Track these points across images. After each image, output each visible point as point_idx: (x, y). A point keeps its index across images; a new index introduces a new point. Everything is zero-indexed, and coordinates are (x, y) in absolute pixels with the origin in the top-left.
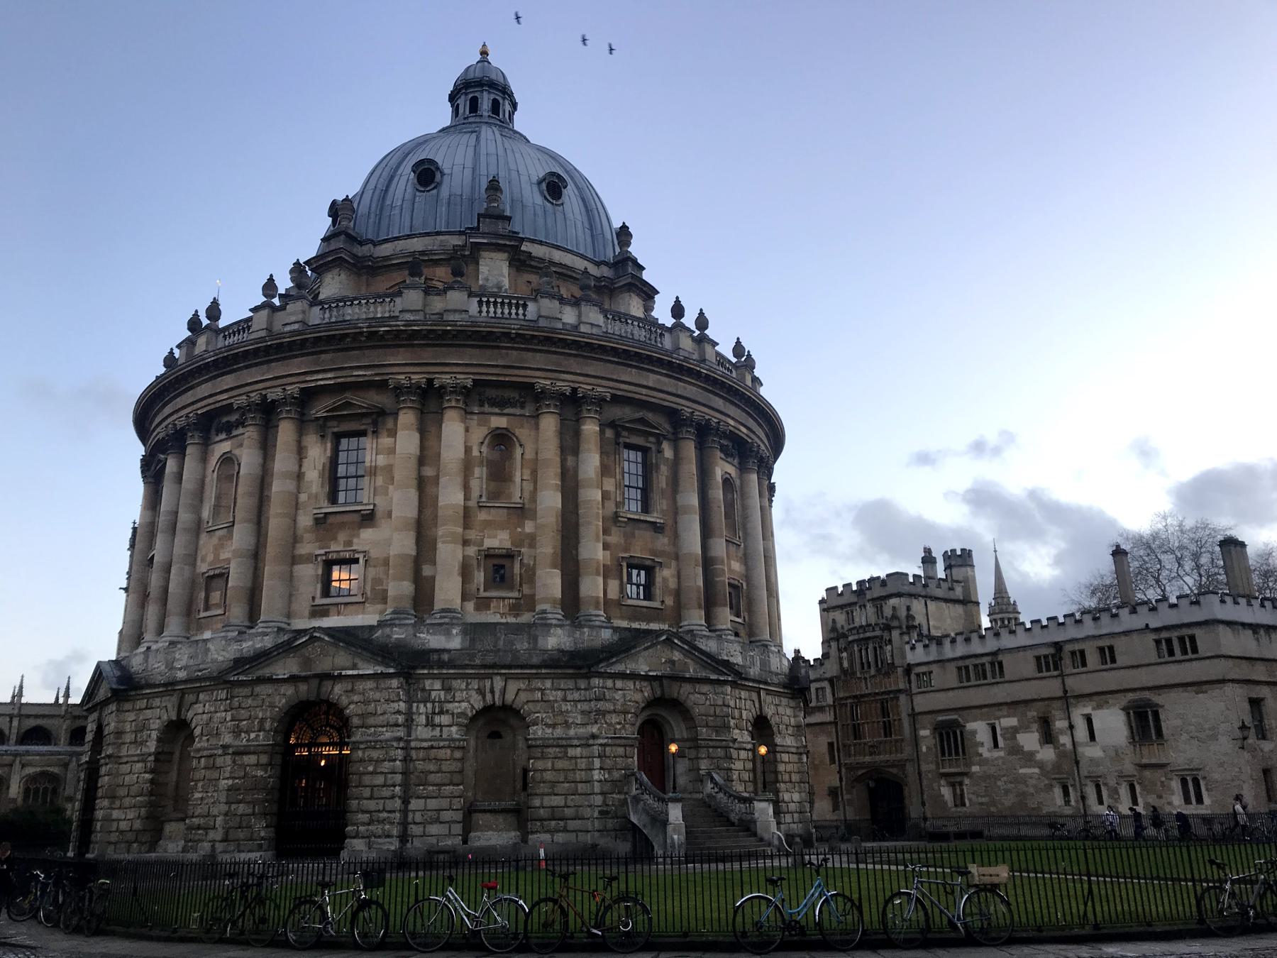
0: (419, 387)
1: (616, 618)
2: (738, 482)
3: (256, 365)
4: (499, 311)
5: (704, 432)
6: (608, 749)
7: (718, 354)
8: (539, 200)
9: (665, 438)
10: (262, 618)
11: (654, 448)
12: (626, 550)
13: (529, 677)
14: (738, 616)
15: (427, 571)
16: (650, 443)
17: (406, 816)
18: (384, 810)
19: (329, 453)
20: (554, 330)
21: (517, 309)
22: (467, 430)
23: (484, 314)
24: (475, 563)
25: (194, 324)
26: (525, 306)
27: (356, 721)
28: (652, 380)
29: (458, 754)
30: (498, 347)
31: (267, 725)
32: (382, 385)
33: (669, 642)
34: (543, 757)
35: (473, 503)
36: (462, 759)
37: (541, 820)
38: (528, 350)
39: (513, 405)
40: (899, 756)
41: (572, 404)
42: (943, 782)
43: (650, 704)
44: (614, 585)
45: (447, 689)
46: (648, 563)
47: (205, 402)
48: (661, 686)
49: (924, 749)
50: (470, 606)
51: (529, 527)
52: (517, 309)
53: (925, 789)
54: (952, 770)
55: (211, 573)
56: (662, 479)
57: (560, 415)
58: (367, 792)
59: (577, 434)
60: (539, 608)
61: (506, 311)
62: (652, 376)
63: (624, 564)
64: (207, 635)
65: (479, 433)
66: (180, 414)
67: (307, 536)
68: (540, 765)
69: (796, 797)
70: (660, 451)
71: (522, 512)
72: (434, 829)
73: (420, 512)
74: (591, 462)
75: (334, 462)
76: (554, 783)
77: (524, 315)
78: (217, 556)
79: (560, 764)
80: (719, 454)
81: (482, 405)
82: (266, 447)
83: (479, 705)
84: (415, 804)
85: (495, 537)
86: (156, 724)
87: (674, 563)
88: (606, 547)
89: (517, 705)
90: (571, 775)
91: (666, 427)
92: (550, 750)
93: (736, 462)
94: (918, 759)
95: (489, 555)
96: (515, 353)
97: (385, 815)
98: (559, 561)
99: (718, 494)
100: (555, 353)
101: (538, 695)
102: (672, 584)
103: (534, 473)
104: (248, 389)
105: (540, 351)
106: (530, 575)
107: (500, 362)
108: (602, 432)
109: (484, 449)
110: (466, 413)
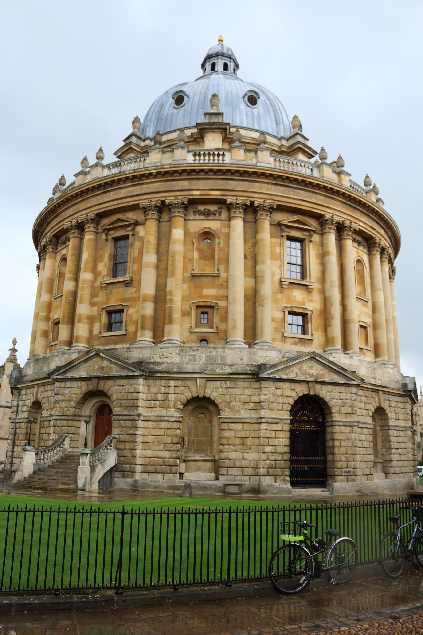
1: (96, 346)
6: (58, 422)
9: (137, 223)
11: (131, 233)
13: (44, 384)
14: (212, 327)
17: (13, 455)
28: (123, 193)
33: (97, 355)
41: (81, 227)
43: (89, 395)
45: (26, 394)
46: (118, 308)
50: (48, 351)
63: (104, 312)
69: (252, 455)
83: (32, 401)
85: (56, 313)
88: (93, 304)
89: (40, 401)
93: (224, 215)
100: (75, 204)
101: (45, 394)
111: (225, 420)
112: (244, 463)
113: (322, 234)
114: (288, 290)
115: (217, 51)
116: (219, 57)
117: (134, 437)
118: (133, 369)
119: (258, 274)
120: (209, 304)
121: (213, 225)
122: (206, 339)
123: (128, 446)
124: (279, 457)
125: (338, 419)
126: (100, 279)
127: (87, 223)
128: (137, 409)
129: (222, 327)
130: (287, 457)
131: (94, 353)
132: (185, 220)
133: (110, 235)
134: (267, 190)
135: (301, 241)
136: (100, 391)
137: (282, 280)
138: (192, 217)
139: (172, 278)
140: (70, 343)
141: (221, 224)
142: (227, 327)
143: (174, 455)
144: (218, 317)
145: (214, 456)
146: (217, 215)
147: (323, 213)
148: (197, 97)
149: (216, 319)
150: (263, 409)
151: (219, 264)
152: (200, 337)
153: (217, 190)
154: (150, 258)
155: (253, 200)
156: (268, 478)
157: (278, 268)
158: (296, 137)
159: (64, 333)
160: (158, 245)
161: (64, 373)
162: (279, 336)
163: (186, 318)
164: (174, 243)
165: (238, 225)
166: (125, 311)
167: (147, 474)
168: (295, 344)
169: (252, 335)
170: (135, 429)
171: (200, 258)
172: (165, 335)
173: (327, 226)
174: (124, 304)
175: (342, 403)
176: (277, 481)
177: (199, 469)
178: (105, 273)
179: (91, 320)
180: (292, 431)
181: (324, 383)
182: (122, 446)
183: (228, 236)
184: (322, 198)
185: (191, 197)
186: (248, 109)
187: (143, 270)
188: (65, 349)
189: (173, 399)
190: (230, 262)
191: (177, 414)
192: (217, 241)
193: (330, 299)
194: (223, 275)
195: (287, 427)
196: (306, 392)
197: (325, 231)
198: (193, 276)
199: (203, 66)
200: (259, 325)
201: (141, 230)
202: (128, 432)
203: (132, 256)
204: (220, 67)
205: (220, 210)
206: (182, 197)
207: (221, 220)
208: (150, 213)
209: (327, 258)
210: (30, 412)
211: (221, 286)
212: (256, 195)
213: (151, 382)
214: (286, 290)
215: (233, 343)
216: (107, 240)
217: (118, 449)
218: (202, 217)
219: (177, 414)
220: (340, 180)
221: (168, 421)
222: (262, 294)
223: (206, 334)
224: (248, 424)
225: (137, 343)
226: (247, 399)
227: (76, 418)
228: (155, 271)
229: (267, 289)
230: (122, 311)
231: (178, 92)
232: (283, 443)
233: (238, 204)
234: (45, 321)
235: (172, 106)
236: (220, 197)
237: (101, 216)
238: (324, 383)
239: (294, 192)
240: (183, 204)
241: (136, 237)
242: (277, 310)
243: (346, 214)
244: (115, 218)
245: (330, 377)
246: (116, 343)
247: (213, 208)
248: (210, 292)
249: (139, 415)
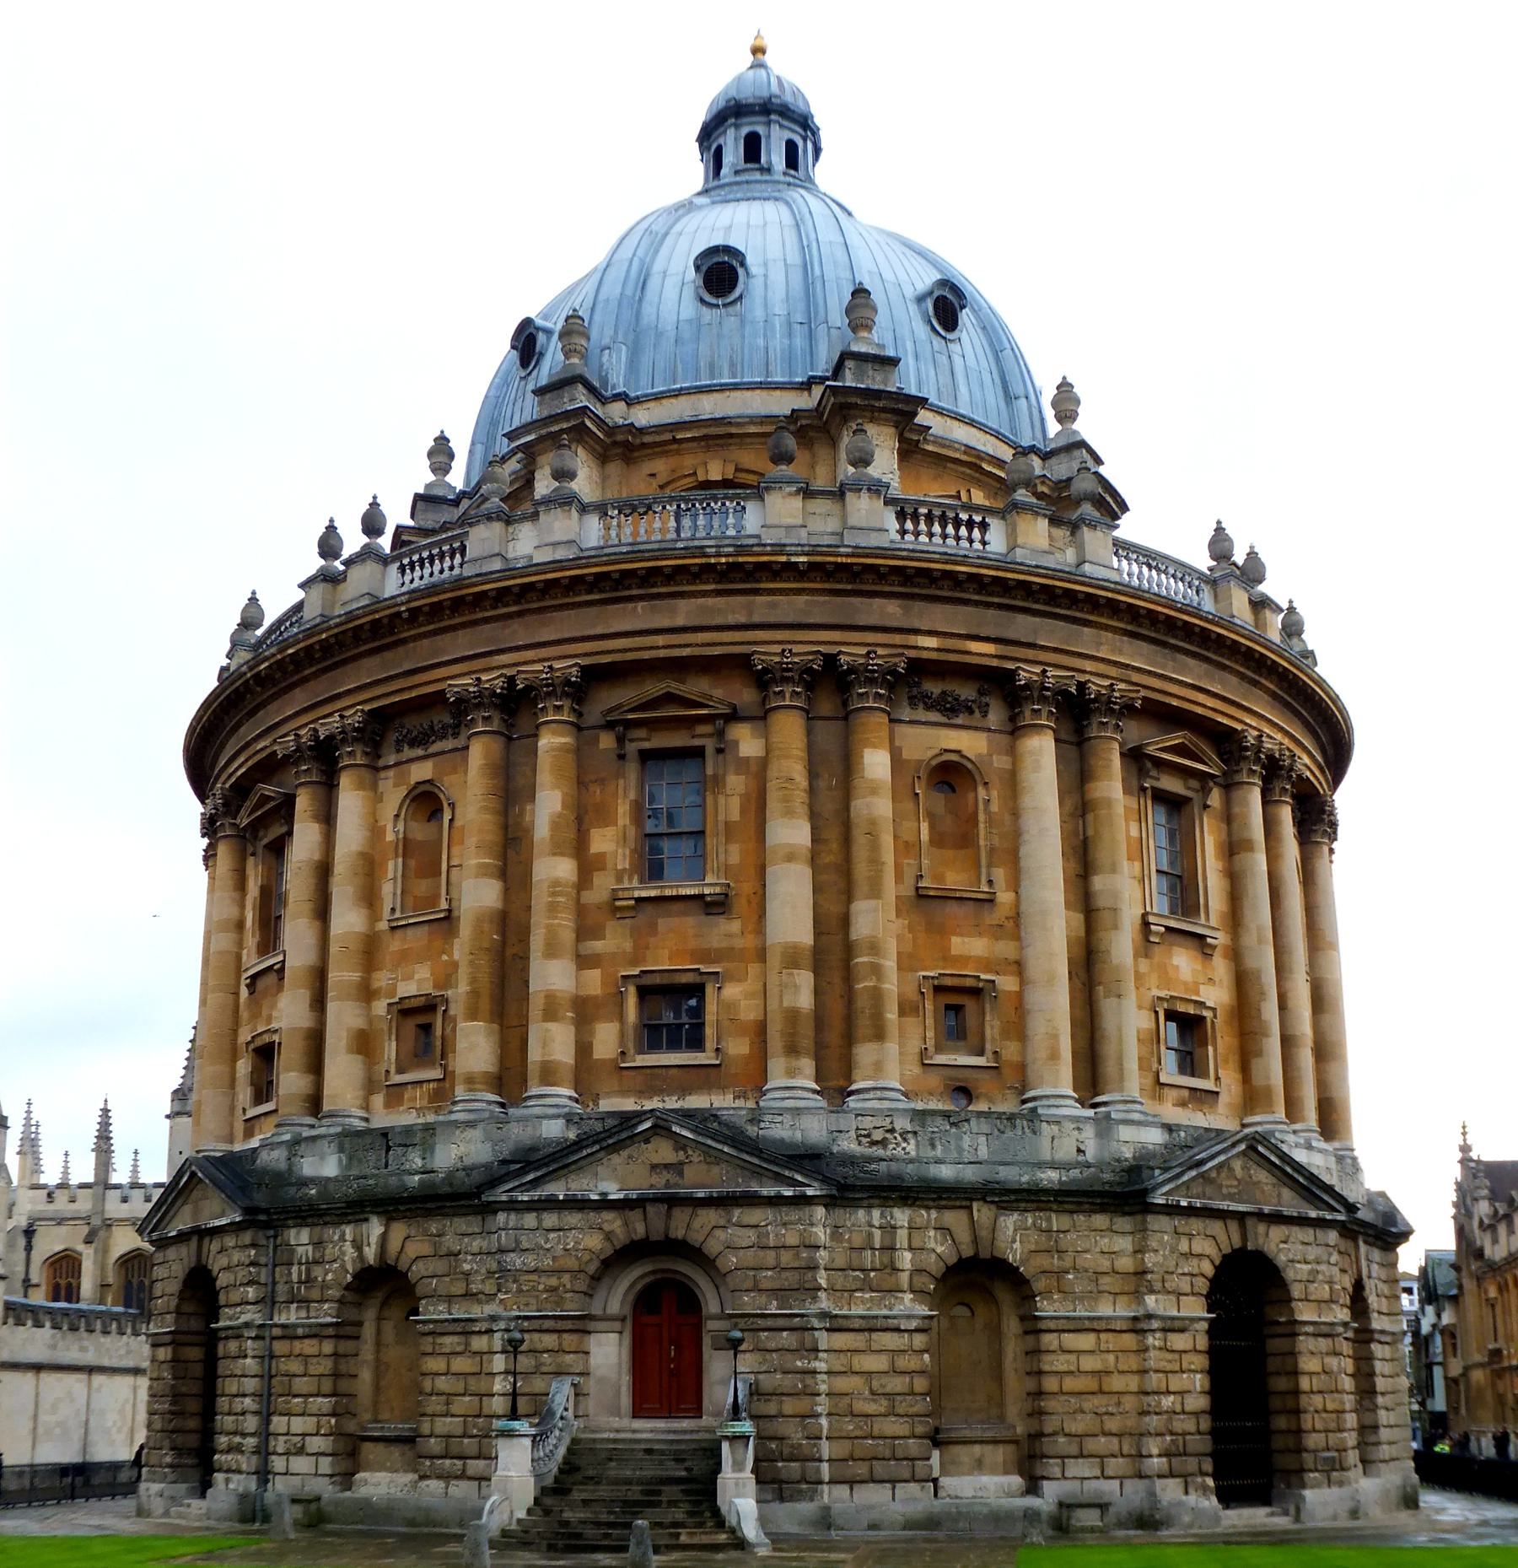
1: (609, 1095)
8: (690, 307)
9: (734, 716)
11: (710, 745)
12: (634, 962)
14: (981, 1053)
16: (702, 738)
28: (683, 612)
39: (443, 737)
56: (730, 804)
62: (683, 605)
63: (632, 990)
65: (393, 795)
79: (461, 1364)
85: (409, 978)
87: (753, 969)
88: (584, 962)
90: (472, 1381)
92: (448, 1340)
93: (996, 716)
96: (426, 642)
98: (485, 1004)
100: (486, 620)
105: (463, 625)
107: (407, 667)
109: (401, 827)
111: (1052, 1325)
112: (1101, 1444)
113: (1229, 786)
114: (1162, 947)
115: (765, 94)
116: (773, 117)
117: (809, 1380)
118: (799, 1178)
119: (1101, 902)
120: (969, 983)
121: (968, 743)
122: (969, 1086)
123: (789, 1406)
124: (1190, 1426)
125: (1305, 1318)
126: (602, 886)
127: (548, 694)
128: (815, 1298)
129: (1010, 1051)
130: (1206, 1423)
131: (647, 1125)
132: (891, 721)
133: (631, 740)
134: (1113, 651)
135: (1173, 804)
136: (676, 1241)
137: (1151, 919)
138: (906, 713)
139: (873, 902)
140: (510, 1080)
141: (989, 741)
142: (1023, 1051)
143: (920, 1430)
144: (997, 1023)
145: (1014, 1427)
146: (977, 714)
147: (1239, 727)
148: (777, 277)
149: (992, 1028)
150: (1152, 1292)
151: (990, 865)
152: (951, 1079)
153: (987, 639)
154: (791, 832)
155: (1083, 678)
156: (1171, 1482)
157: (1136, 884)
158: (1076, 453)
159: (474, 1047)
160: (812, 791)
161: (535, 1183)
162: (1149, 1081)
163: (912, 1022)
164: (874, 791)
165: (1042, 751)
166: (710, 991)
167: (846, 1488)
168: (1182, 1104)
169: (1092, 1077)
170: (813, 1356)
171: (931, 841)
172: (856, 1074)
173: (1244, 766)
174: (703, 969)
175: (1311, 1272)
176: (1191, 1490)
177: (979, 1466)
178: (623, 863)
179: (584, 1012)
180: (1212, 1352)
181: (1277, 1218)
182: (771, 1408)
183: (1013, 783)
184: (1235, 680)
185: (912, 654)
186: (937, 341)
187: (768, 870)
188: (489, 1103)
189: (908, 1266)
190: (1023, 863)
191: (923, 1310)
192: (982, 793)
193: (1259, 978)
194: (1005, 897)
195: (1203, 1342)
196: (1237, 1242)
197: (1237, 778)
198: (921, 896)
199: (708, 135)
200: (1109, 1050)
201: (747, 742)
202: (789, 1366)
203: (721, 817)
204: (775, 156)
205: (985, 699)
206: (885, 653)
207: (989, 730)
208: (788, 689)
209: (1242, 858)
210: (341, 1301)
211: (998, 932)
212: (1088, 666)
213: (840, 1214)
214: (1156, 949)
215: (1052, 1102)
216: (622, 757)
217: (752, 1417)
218: (934, 716)
219: (923, 1310)
220: (1259, 623)
221: (898, 1330)
222: (1115, 962)
223: (967, 1073)
224: (1110, 1335)
225: (769, 1096)
226: (1105, 1264)
227: (582, 1325)
228: (808, 871)
229: (1122, 945)
230: (698, 990)
231: (714, 250)
232: (1195, 1383)
233: (1048, 689)
234: (358, 1000)
235: (689, 294)
236: (995, 663)
237: (596, 676)
238: (1277, 1218)
239: (1174, 660)
240: (893, 672)
241: (729, 757)
242: (1140, 1007)
243: (1281, 729)
244: (654, 688)
245: (1290, 1203)
246: (684, 1091)
247: (966, 692)
248: (971, 947)
249: (824, 1315)
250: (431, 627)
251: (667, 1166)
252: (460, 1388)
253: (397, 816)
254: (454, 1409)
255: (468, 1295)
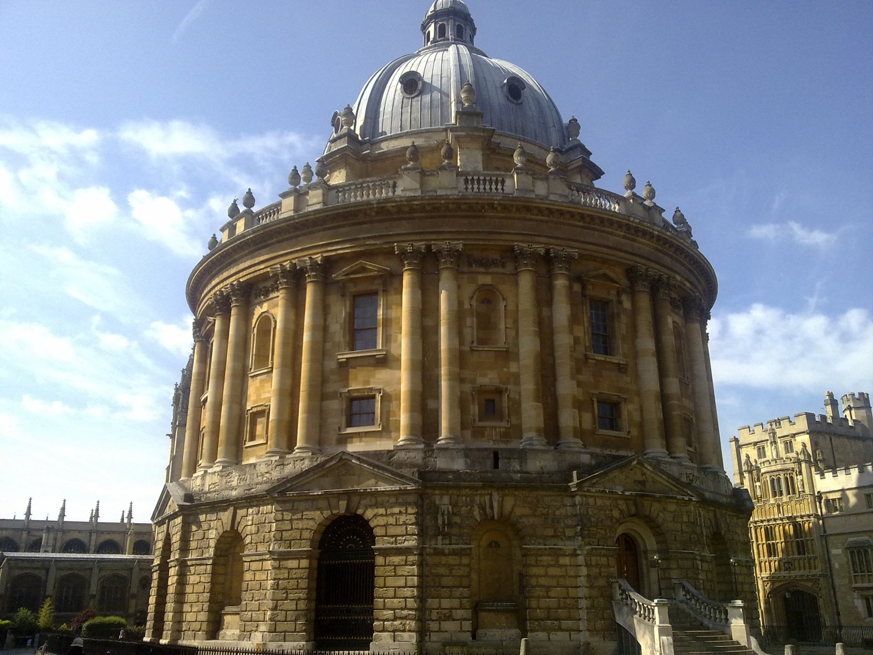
0: (420, 253)
2: (684, 331)
3: (287, 239)
4: (482, 187)
5: (656, 287)
6: (593, 558)
7: (664, 220)
9: (624, 291)
10: (298, 445)
14: (690, 446)
15: (431, 404)
18: (406, 608)
19: (348, 310)
20: (528, 200)
21: (497, 184)
22: (459, 287)
23: (470, 190)
24: (470, 398)
25: (234, 211)
26: (503, 182)
27: (378, 531)
29: (465, 560)
30: (483, 217)
31: (307, 534)
32: (390, 253)
34: (536, 566)
35: (466, 348)
36: (468, 565)
37: (538, 620)
38: (509, 218)
40: (813, 572)
42: (856, 595)
44: (587, 418)
46: (615, 398)
47: (245, 273)
48: (636, 504)
49: (837, 566)
50: (468, 434)
51: (513, 367)
52: (497, 184)
53: (840, 601)
54: (866, 585)
55: (255, 410)
56: (622, 327)
57: (536, 272)
58: (391, 592)
59: (551, 288)
60: (526, 435)
61: (488, 187)
63: (595, 400)
64: (252, 460)
65: (469, 289)
66: (225, 283)
67: (332, 377)
68: (535, 571)
70: (620, 302)
71: (508, 355)
72: (449, 626)
73: (424, 355)
74: (562, 312)
75: (351, 317)
76: (548, 588)
77: (503, 189)
78: (259, 396)
80: (670, 307)
81: (470, 265)
82: (296, 305)
84: (432, 602)
85: (485, 375)
86: (213, 534)
87: (636, 399)
88: (579, 384)
90: (561, 580)
91: (625, 282)
92: (545, 558)
93: (681, 312)
94: (829, 573)
95: (481, 391)
97: (405, 612)
99: (669, 340)
102: (637, 417)
103: (516, 322)
104: (282, 259)
106: (516, 407)
107: (486, 230)
108: (570, 287)
109: (474, 303)
110: (458, 272)
154: (647, 343)
246: (618, 448)
250: (503, 215)
251: (640, 482)
252: (554, 583)
253: (472, 298)
254: (551, 594)
255: (555, 536)
